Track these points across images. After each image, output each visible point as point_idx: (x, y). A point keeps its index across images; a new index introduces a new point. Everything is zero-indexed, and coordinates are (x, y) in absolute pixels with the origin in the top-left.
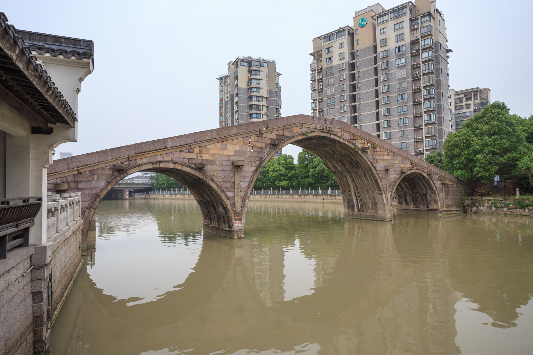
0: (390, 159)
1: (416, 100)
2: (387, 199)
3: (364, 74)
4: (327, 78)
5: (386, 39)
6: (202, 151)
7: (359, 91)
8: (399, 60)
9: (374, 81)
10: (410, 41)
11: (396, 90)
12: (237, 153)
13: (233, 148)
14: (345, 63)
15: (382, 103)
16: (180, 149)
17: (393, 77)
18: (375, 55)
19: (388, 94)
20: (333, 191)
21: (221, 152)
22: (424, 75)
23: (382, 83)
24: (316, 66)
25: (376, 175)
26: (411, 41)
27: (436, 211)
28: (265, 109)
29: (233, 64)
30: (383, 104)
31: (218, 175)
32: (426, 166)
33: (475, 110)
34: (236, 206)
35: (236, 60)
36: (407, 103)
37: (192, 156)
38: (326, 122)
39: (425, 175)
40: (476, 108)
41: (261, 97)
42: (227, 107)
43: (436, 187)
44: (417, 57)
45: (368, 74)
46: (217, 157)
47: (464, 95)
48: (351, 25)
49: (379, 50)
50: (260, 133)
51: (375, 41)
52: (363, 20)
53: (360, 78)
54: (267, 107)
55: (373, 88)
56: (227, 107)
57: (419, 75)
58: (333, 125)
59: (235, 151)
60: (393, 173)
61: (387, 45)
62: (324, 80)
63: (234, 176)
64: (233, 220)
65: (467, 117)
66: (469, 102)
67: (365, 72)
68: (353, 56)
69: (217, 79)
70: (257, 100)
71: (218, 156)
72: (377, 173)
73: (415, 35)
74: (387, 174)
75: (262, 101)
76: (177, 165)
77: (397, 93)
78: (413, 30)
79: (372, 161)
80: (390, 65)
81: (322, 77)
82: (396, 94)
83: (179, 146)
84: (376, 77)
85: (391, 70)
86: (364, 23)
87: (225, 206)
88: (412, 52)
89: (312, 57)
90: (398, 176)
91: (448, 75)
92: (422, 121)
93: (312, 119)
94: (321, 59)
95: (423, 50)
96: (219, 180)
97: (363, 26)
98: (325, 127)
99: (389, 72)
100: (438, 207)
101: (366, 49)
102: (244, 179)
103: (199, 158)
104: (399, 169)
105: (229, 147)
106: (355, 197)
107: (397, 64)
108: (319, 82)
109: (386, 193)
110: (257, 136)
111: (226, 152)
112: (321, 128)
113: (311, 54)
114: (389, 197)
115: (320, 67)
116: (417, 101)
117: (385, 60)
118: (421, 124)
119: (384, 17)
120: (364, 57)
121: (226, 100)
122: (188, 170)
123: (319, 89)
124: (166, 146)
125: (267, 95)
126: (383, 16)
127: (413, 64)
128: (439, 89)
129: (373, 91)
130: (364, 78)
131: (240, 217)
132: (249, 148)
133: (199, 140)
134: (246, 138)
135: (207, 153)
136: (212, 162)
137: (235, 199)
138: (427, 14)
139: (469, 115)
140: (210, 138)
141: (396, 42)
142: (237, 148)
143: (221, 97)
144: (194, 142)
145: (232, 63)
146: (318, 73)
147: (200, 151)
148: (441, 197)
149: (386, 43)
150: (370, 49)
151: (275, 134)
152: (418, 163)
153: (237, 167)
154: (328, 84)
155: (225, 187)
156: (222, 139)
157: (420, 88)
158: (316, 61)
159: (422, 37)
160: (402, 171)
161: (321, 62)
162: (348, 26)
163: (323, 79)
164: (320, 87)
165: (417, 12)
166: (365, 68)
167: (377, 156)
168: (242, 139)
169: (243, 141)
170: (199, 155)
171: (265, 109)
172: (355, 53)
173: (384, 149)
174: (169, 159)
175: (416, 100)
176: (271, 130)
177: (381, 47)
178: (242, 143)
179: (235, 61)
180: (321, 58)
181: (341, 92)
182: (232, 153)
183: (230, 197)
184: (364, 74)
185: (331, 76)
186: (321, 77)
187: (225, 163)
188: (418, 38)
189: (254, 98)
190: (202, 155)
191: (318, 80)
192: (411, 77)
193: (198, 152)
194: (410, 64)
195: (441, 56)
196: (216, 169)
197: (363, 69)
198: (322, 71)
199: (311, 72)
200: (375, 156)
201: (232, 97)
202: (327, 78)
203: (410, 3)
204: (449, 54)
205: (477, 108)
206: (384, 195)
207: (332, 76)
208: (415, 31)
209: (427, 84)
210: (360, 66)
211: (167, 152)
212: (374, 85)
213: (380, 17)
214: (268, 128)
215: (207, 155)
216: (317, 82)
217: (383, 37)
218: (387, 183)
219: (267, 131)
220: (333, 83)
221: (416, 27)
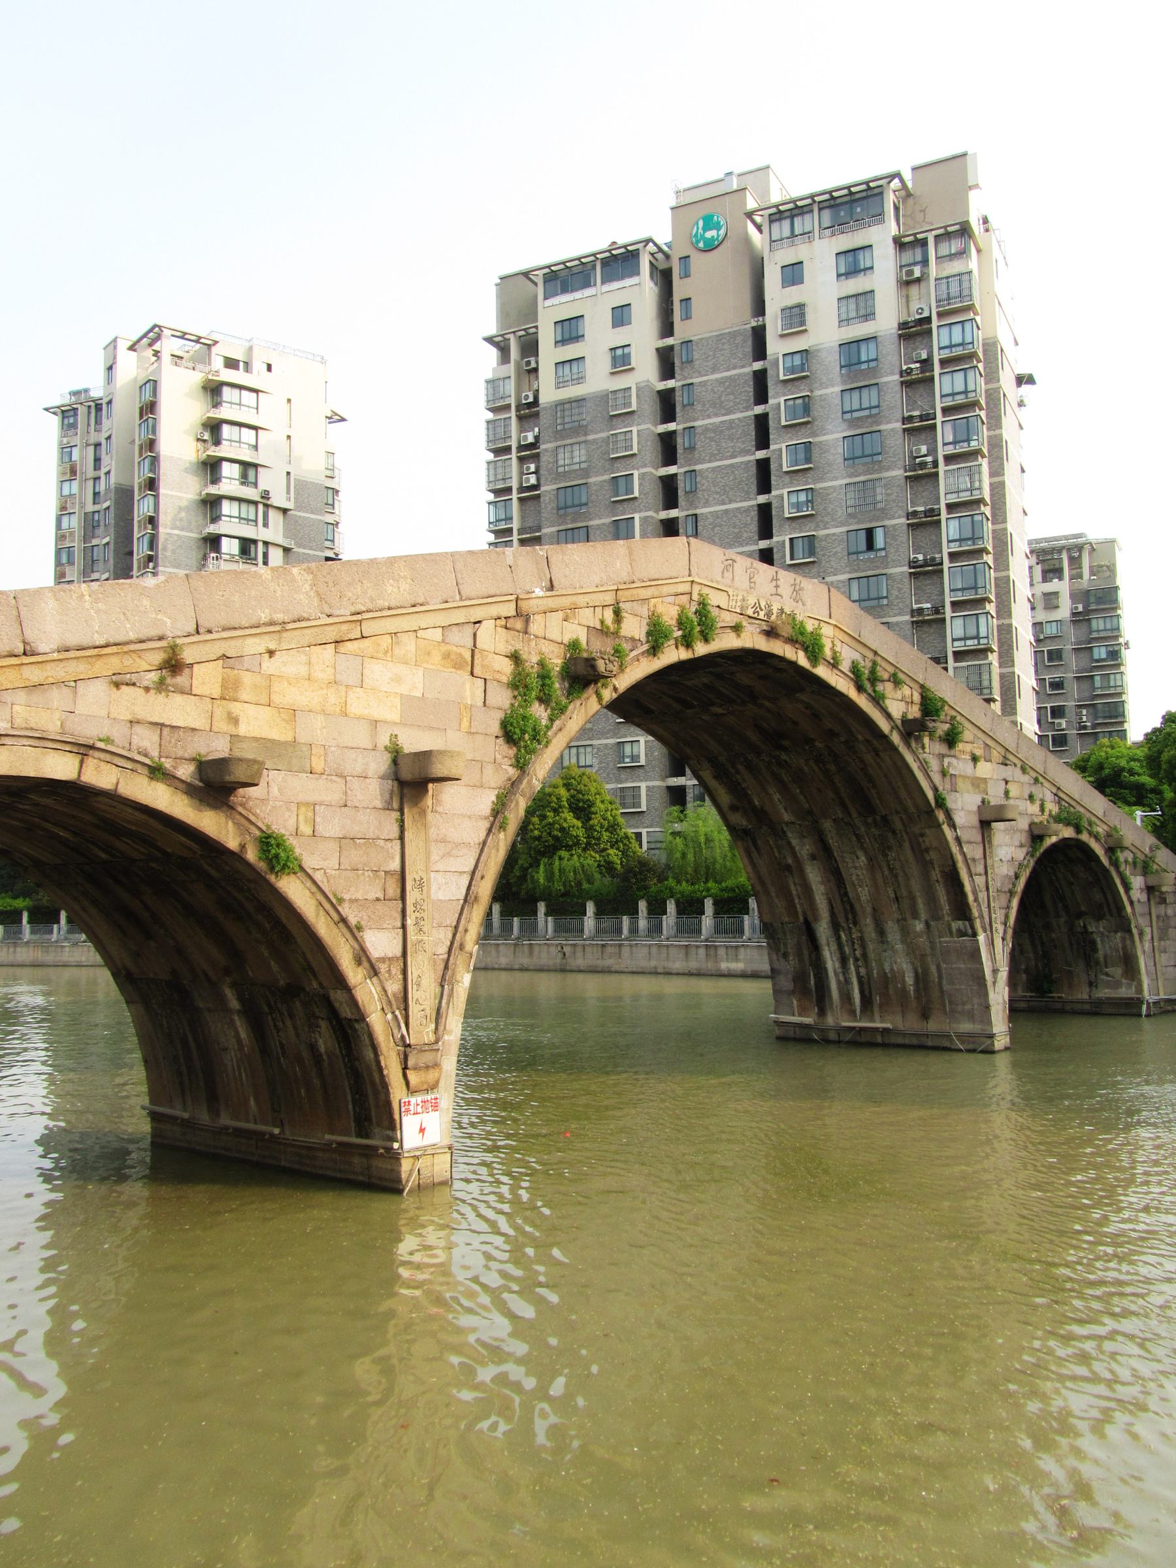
0: (995, 777)
1: (920, 557)
2: (993, 960)
3: (712, 439)
4: (559, 443)
5: (801, 306)
6: (237, 685)
7: (692, 505)
8: (856, 394)
9: (753, 470)
10: (896, 326)
11: (840, 513)
13: (397, 679)
14: (638, 389)
15: (789, 562)
16: (114, 664)
17: (831, 458)
18: (758, 366)
19: (813, 526)
20: (608, 922)
21: (333, 698)
22: (949, 459)
23: (787, 479)
24: (511, 387)
25: (955, 849)
26: (899, 324)
27: (1130, 1008)
28: (276, 556)
29: (132, 348)
30: (791, 565)
31: (320, 829)
32: (1100, 814)
33: (1074, 614)
34: (414, 1009)
35: (151, 330)
36: (886, 567)
38: (777, 587)
39: (1099, 850)
40: (1076, 608)
41: (261, 507)
42: (95, 542)
43: (1131, 903)
44: (921, 389)
45: (731, 438)
46: (313, 730)
47: (1038, 557)
48: (663, 235)
49: (775, 347)
50: (519, 614)
51: (759, 308)
52: (709, 224)
53: (697, 456)
54: (287, 550)
55: (750, 499)
56: (95, 542)
57: (929, 459)
58: (804, 605)
59: (406, 700)
60: (1007, 839)
61: (805, 331)
62: (546, 450)
63: (402, 838)
64: (397, 1092)
65: (1048, 641)
66: (1054, 585)
67: (716, 429)
68: (667, 363)
69: (47, 409)
70: (240, 518)
71: (319, 720)
72: (958, 840)
73: (914, 306)
74: (990, 842)
75: (266, 525)
76: (90, 763)
77: (842, 524)
78: (908, 283)
79: (937, 778)
80: (816, 410)
81: (537, 438)
82: (844, 529)
83: (107, 646)
84: (761, 454)
85: (823, 431)
86: (713, 233)
87: (346, 1012)
88: (904, 368)
89: (493, 353)
90: (1020, 854)
91: (1023, 471)
92: (945, 642)
94: (533, 365)
95: (944, 362)
97: (710, 248)
98: (775, 611)
99: (817, 439)
100: (1140, 989)
101: (720, 338)
102: (449, 854)
103: (221, 725)
104: (1023, 824)
105: (378, 673)
106: (834, 947)
107: (847, 408)
108: (521, 460)
109: (989, 928)
110: (506, 628)
111: (359, 704)
112: (762, 615)
113: (489, 340)
114: (998, 942)
115: (527, 397)
116: (925, 560)
117: (801, 391)
118: (940, 652)
119: (797, 221)
120: (714, 370)
121: (90, 508)
123: (522, 489)
124: (30, 635)
125: (289, 499)
126: (792, 217)
127: (906, 415)
128: (1001, 519)
129: (748, 510)
130: (715, 455)
131: (431, 1076)
132: (468, 686)
133: (222, 618)
134: (454, 628)
135: (265, 700)
137: (404, 972)
138: (957, 227)
139: (1054, 631)
140: (279, 617)
141: (844, 321)
142: (415, 682)
143: (66, 492)
144: (191, 628)
145: (130, 343)
146: (520, 418)
147: (224, 686)
148: (1147, 945)
149: (803, 323)
150: (739, 339)
151: (585, 622)
152: (1076, 797)
154: (561, 470)
155: (356, 900)
156: (344, 627)
157: (932, 510)
158: (511, 369)
159: (940, 315)
160: (1036, 832)
161: (532, 376)
162: (648, 241)
163: (543, 447)
164: (528, 480)
165: (919, 217)
166: (716, 415)
167: (954, 761)
168: (437, 635)
169: (444, 648)
170: (220, 710)
171: (276, 556)
172: (677, 349)
173: (976, 731)
174: (51, 724)
175: (920, 557)
176: (566, 602)
177: (782, 336)
178: (437, 657)
179: (145, 336)
180: (532, 360)
181: (620, 507)
182: (390, 712)
183: (383, 960)
184: (712, 439)
185: (578, 434)
186: (531, 439)
187: (354, 764)
188: (926, 314)
189: (227, 508)
190: (236, 708)
191: (521, 448)
192: (900, 463)
193: (216, 693)
194: (899, 416)
195: (1004, 395)
196: (312, 798)
197: (709, 417)
198: (537, 415)
199: (490, 416)
201: (124, 498)
202: (559, 443)
203: (896, 180)
204: (1025, 388)
205: (1080, 608)
206: (981, 938)
207: (582, 439)
208: (914, 290)
209: (961, 494)
210: (699, 407)
211: (34, 674)
212: (754, 488)
213: (780, 220)
214: (551, 587)
215: (266, 712)
216: (514, 455)
217: (793, 295)
218: (990, 883)
219: (551, 603)
220: (583, 466)
221: (917, 272)
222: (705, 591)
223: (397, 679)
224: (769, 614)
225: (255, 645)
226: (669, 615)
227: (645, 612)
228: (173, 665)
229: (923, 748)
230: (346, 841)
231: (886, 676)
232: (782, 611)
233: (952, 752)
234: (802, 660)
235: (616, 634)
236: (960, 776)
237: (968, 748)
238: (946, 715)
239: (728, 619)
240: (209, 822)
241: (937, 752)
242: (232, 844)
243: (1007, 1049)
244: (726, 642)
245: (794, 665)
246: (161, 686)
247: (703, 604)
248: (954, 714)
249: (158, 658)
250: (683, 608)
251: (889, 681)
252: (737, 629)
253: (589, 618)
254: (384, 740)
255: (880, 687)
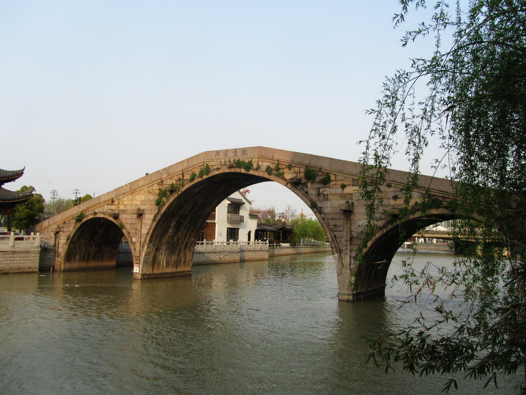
12: (143, 202)
16: (106, 203)
21: (131, 202)
37: (113, 207)
46: (128, 207)
59: (142, 201)
71: (129, 206)
93: (217, 155)
96: (128, 227)
103: (118, 209)
105: (137, 197)
111: (135, 203)
122: (111, 219)
136: (124, 211)
142: (143, 198)
151: (175, 179)
153: (140, 215)
167: (328, 189)
174: (101, 211)
176: (170, 176)
178: (146, 193)
200: (321, 190)
215: (123, 206)
222: (207, 163)
223: (140, 198)
224: (230, 161)
225: (121, 197)
226: (197, 171)
227: (191, 173)
228: (113, 201)
229: (307, 187)
230: (131, 224)
231: (284, 167)
232: (235, 160)
233: (327, 186)
234: (243, 171)
235: (183, 179)
236: (331, 194)
237: (340, 183)
238: (323, 172)
239: (216, 167)
240: (115, 221)
241: (316, 187)
242: (118, 225)
243: (348, 301)
244: (217, 173)
245: (240, 174)
246: (112, 204)
247: (207, 165)
248: (329, 172)
249: (111, 201)
250: (202, 169)
251: (286, 168)
252: (218, 169)
253: (176, 178)
254: (137, 208)
255: (281, 171)
